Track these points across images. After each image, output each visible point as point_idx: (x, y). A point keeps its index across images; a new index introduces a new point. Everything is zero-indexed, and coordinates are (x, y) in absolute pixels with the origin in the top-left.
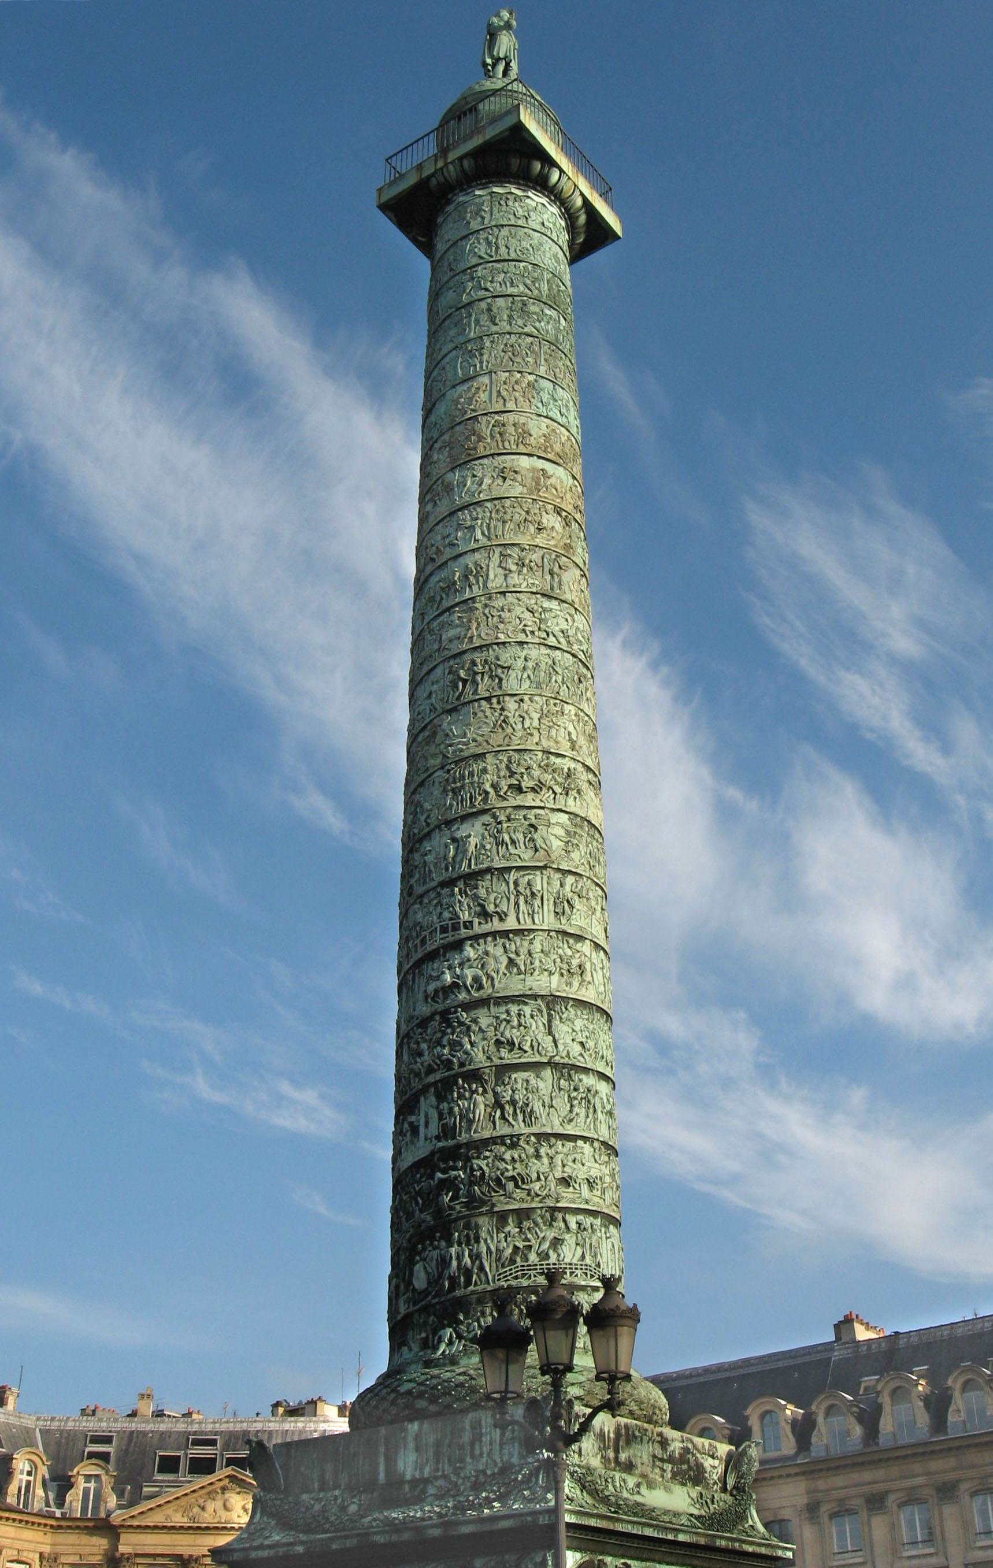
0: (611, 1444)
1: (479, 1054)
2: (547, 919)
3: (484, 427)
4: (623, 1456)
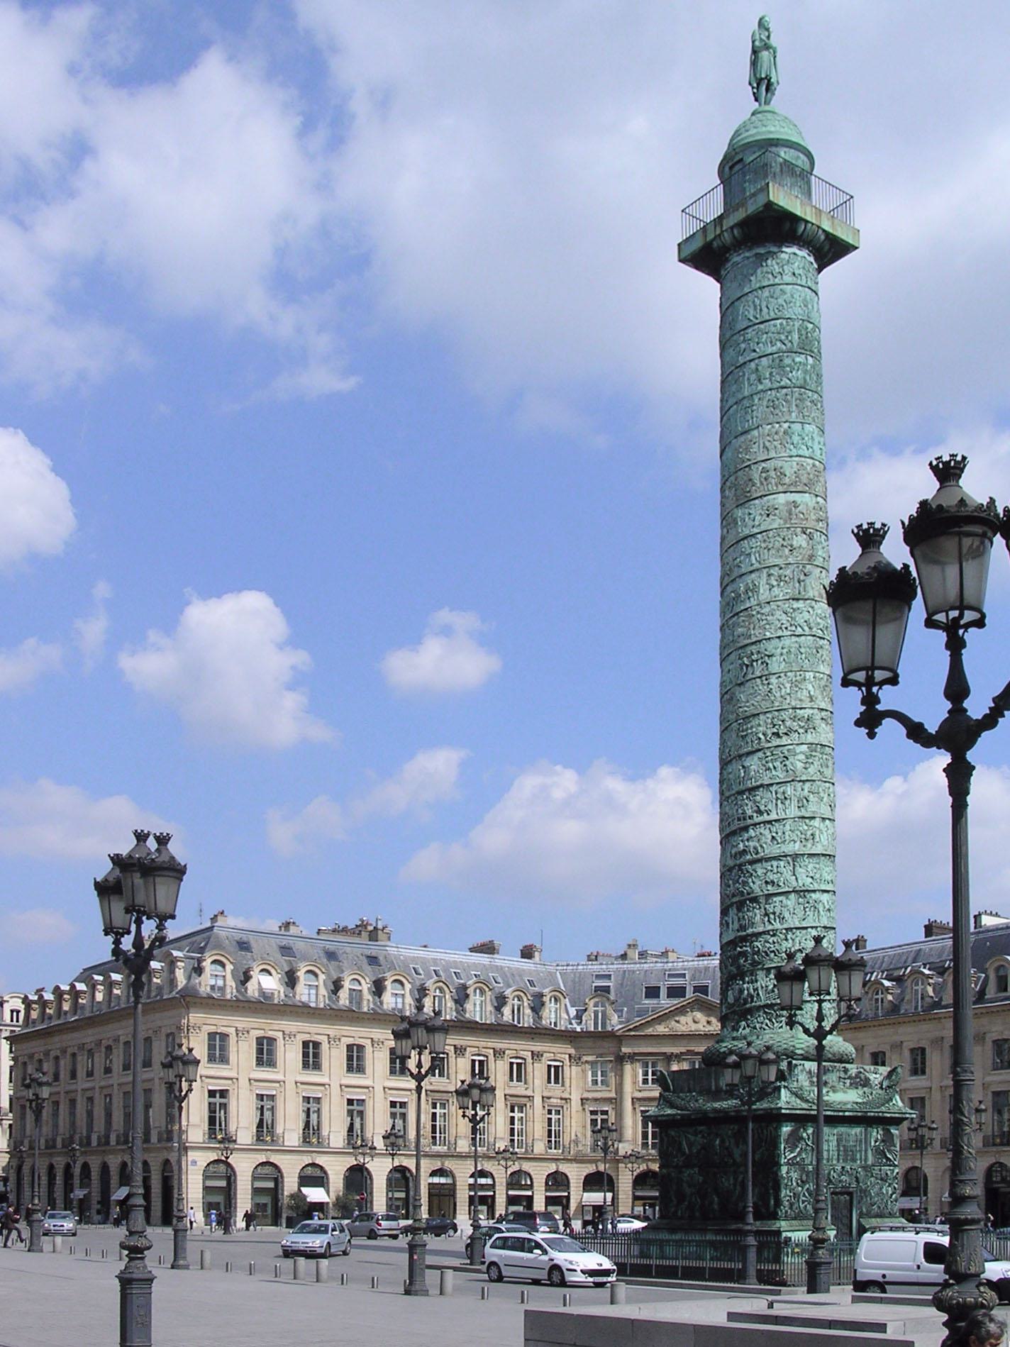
1: (757, 887)
2: (793, 811)
3: (756, 474)
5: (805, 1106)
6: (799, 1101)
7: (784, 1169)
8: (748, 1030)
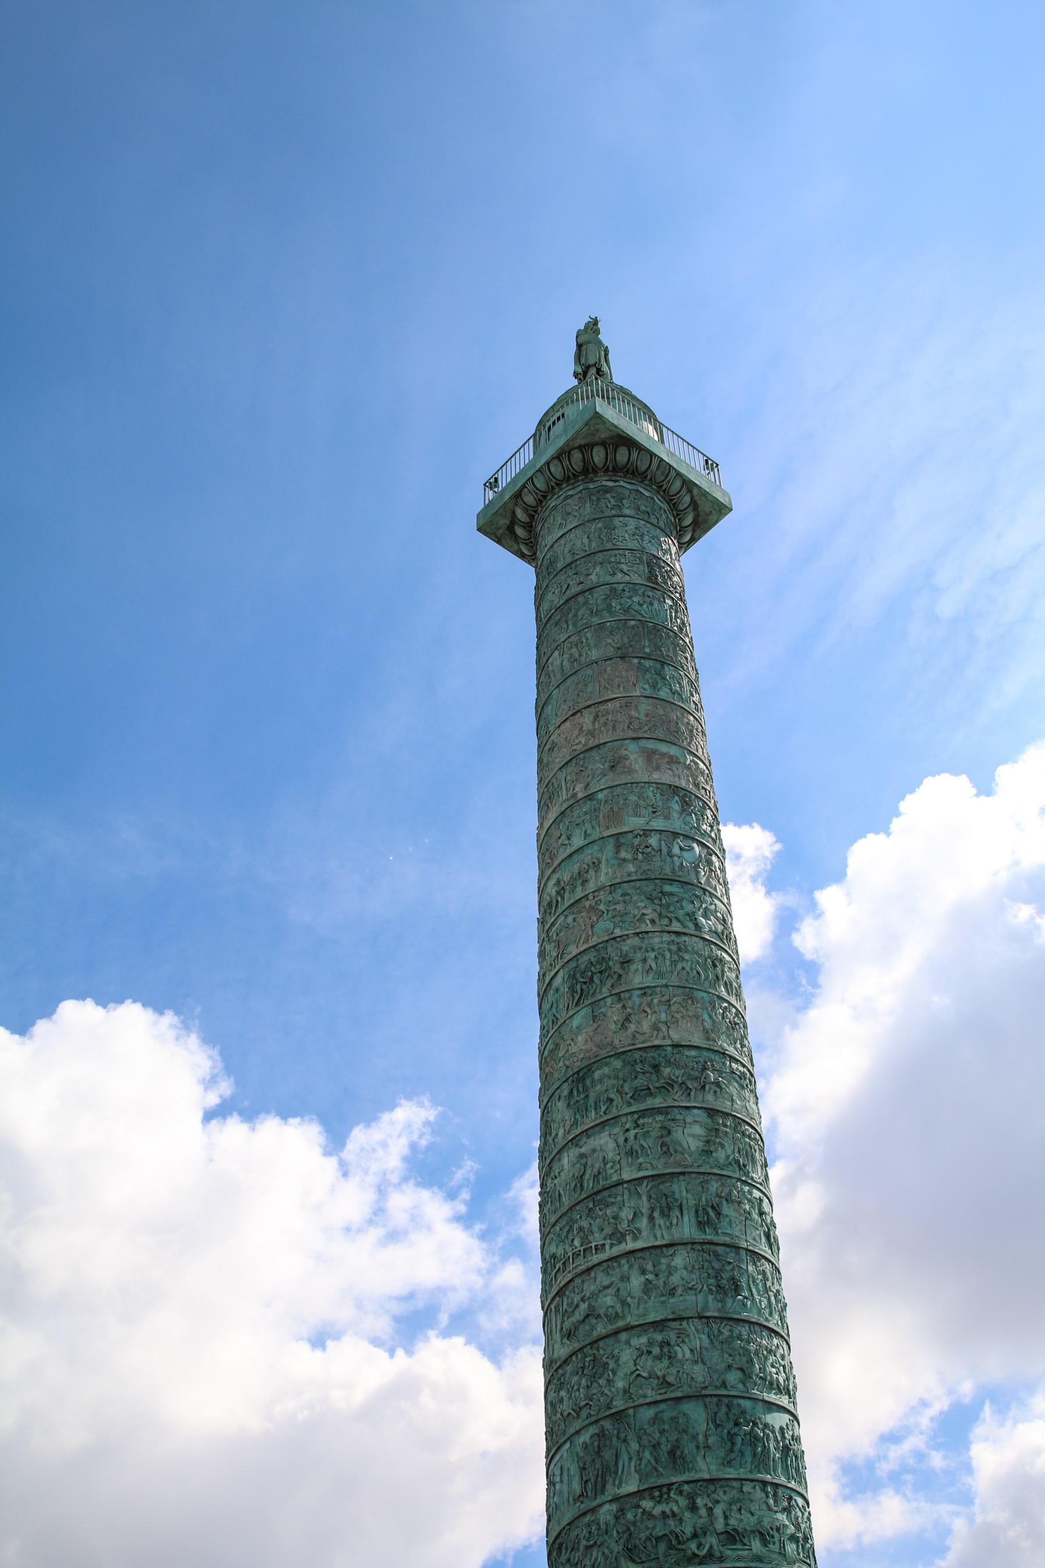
2: (687, 1228)
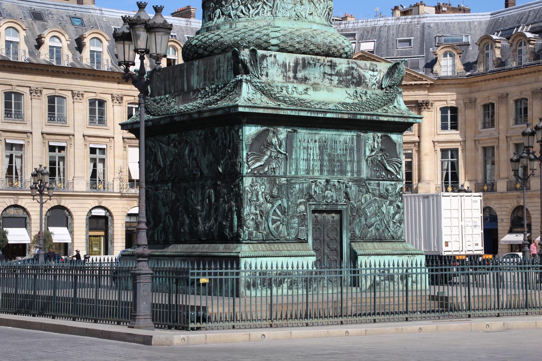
0: (291, 69)
4: (300, 75)
5: (272, 104)
6: (265, 99)
7: (247, 182)
8: (222, 19)
